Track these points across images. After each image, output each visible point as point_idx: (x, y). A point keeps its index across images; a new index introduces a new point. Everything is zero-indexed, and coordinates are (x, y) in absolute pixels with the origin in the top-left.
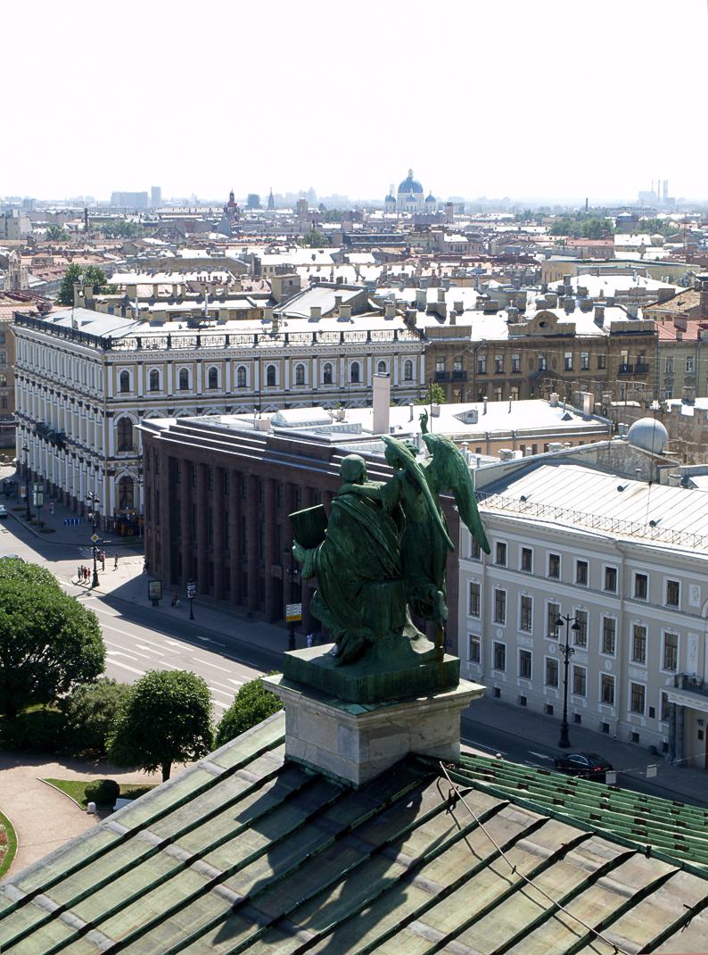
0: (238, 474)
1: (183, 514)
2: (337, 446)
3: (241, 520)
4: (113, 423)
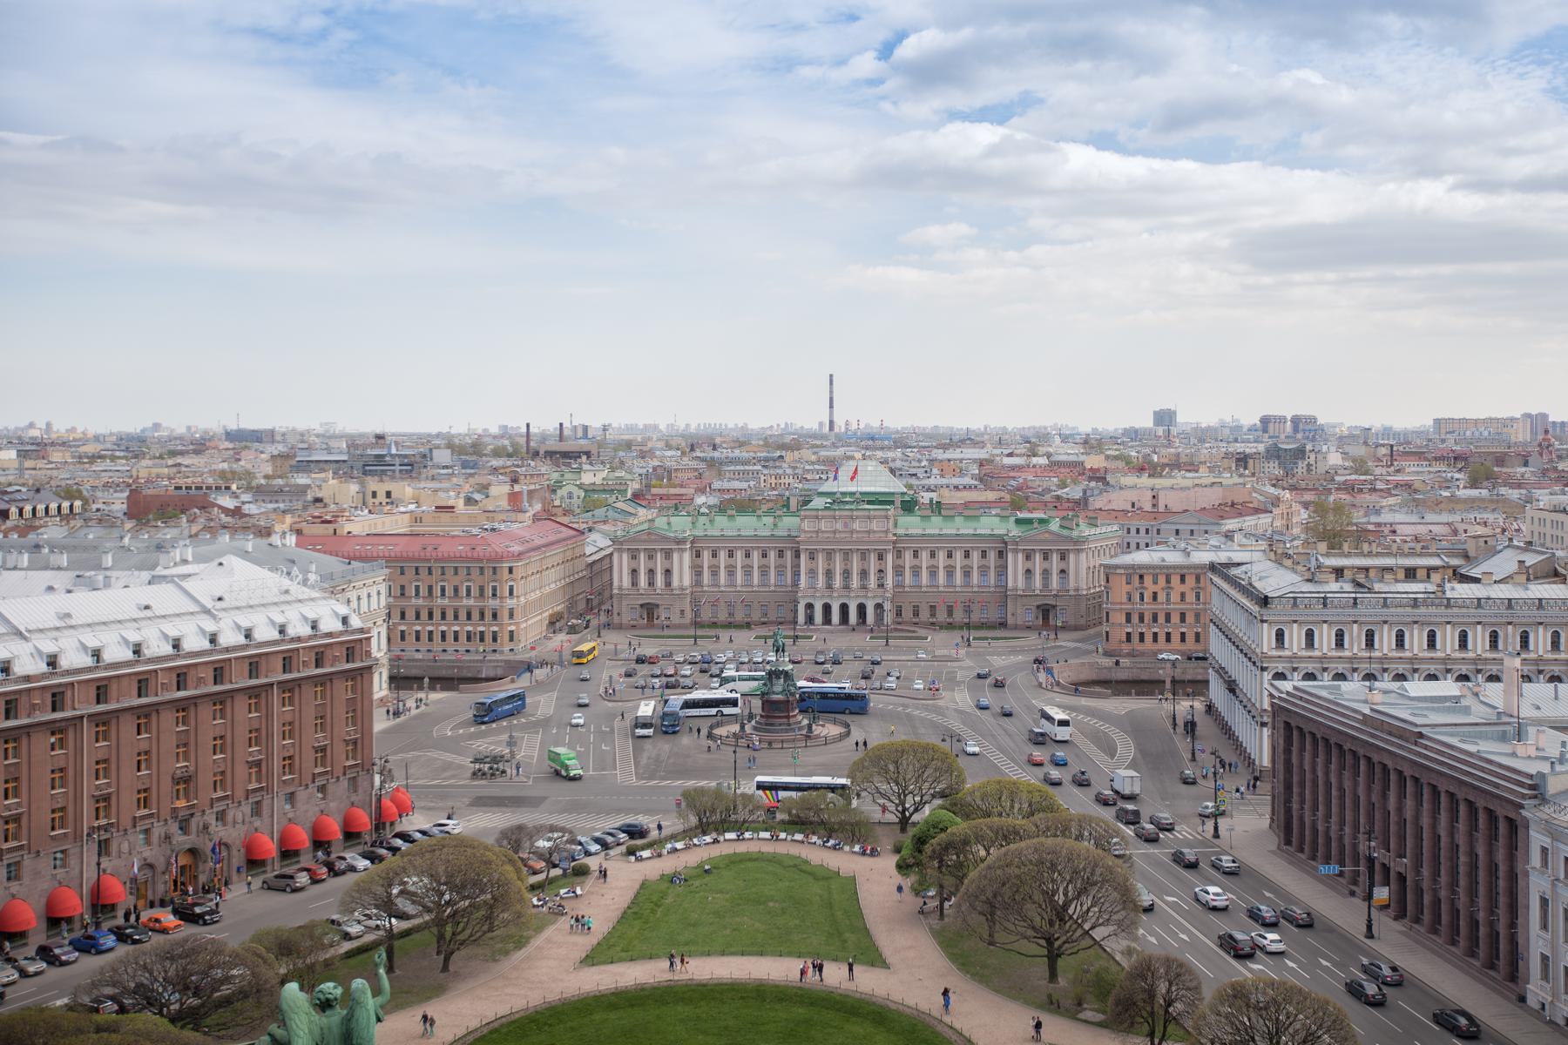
0: (1340, 747)
1: (1295, 779)
2: (1424, 731)
3: (1341, 790)
4: (1267, 676)
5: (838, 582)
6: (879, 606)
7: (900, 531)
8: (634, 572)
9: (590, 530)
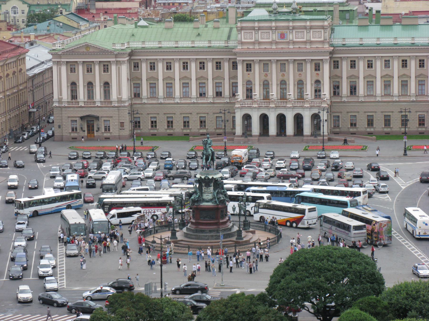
5: (274, 92)
6: (316, 117)
7: (337, 42)
8: (73, 85)
9: (32, 44)
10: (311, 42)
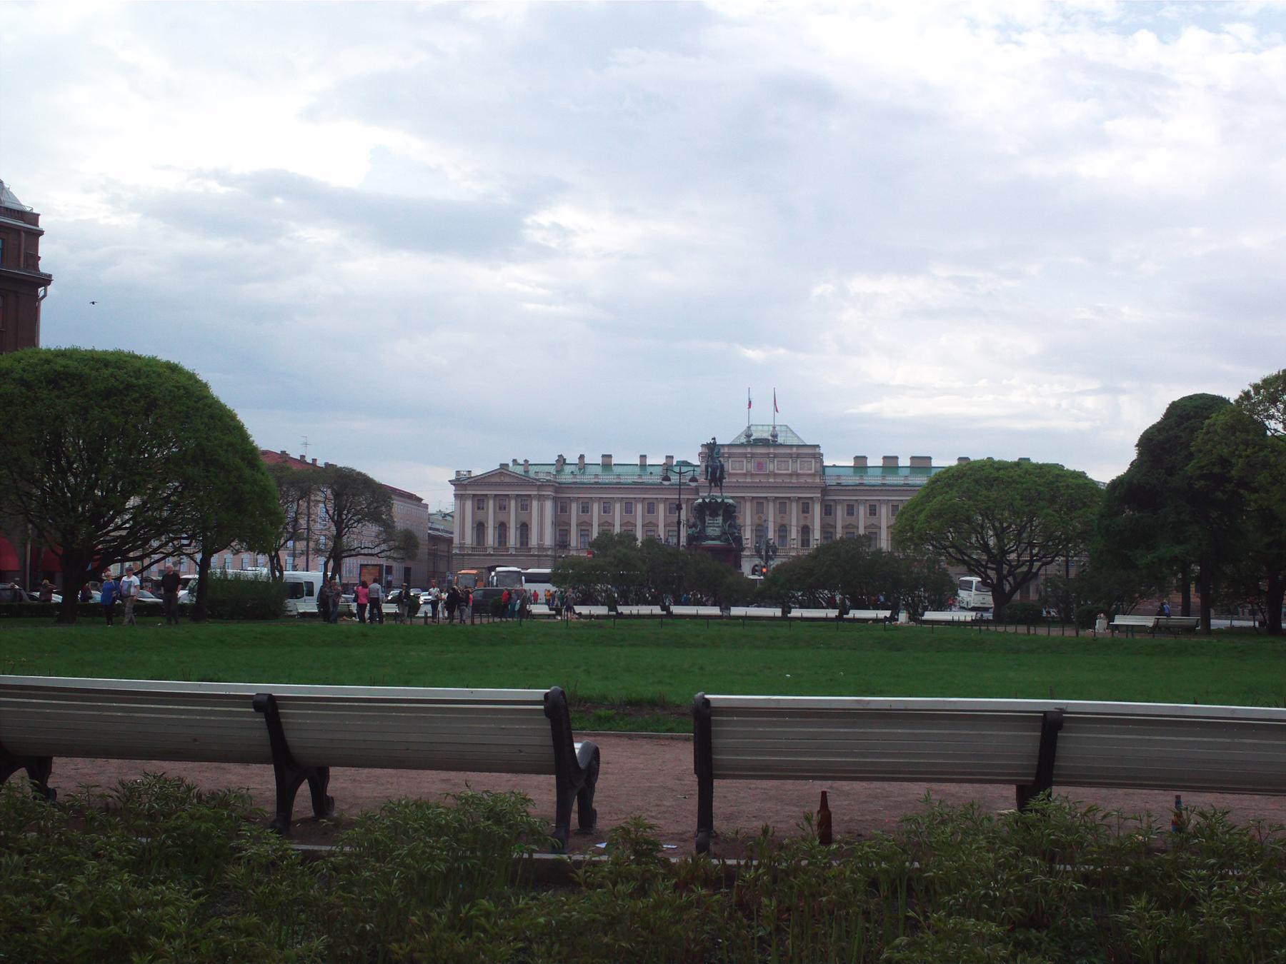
8: (480, 527)
10: (798, 475)
